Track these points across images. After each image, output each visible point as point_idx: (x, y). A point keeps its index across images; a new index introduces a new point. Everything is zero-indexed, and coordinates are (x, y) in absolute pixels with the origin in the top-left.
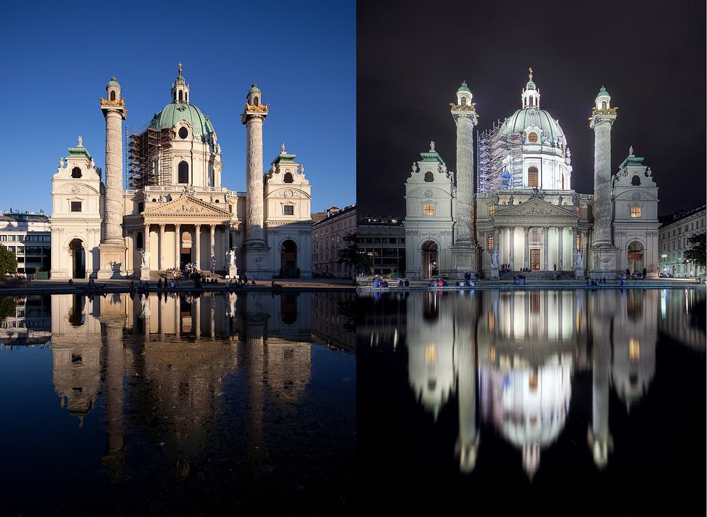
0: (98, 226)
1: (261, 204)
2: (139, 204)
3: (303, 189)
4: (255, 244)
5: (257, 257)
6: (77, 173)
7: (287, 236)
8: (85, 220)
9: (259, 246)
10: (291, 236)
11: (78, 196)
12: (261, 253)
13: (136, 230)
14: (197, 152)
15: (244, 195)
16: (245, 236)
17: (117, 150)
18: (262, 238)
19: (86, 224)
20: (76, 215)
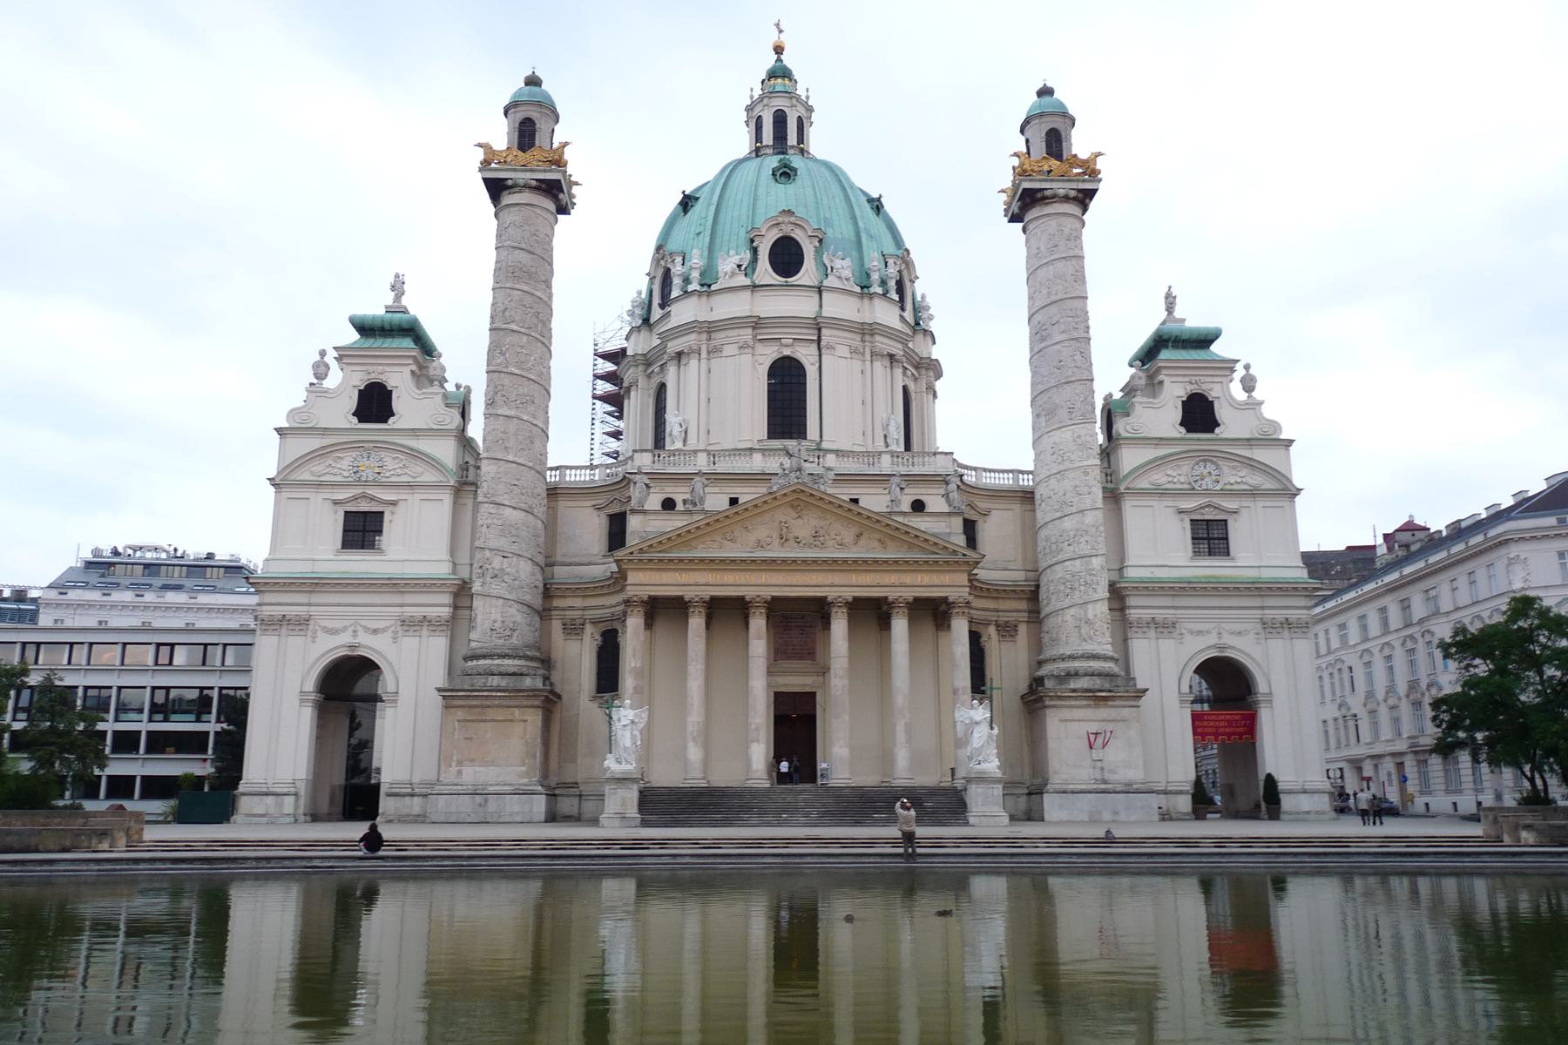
0: (439, 605)
1: (1096, 518)
2: (612, 517)
3: (1260, 454)
4: (1076, 674)
5: (1094, 728)
6: (374, 404)
7: (1212, 640)
8: (395, 585)
9: (1097, 683)
10: (1229, 640)
11: (370, 492)
12: (1103, 712)
13: (594, 622)
14: (839, 324)
15: (1026, 482)
16: (1037, 645)
17: (534, 320)
18: (1108, 649)
19: (397, 599)
20: (360, 563)
